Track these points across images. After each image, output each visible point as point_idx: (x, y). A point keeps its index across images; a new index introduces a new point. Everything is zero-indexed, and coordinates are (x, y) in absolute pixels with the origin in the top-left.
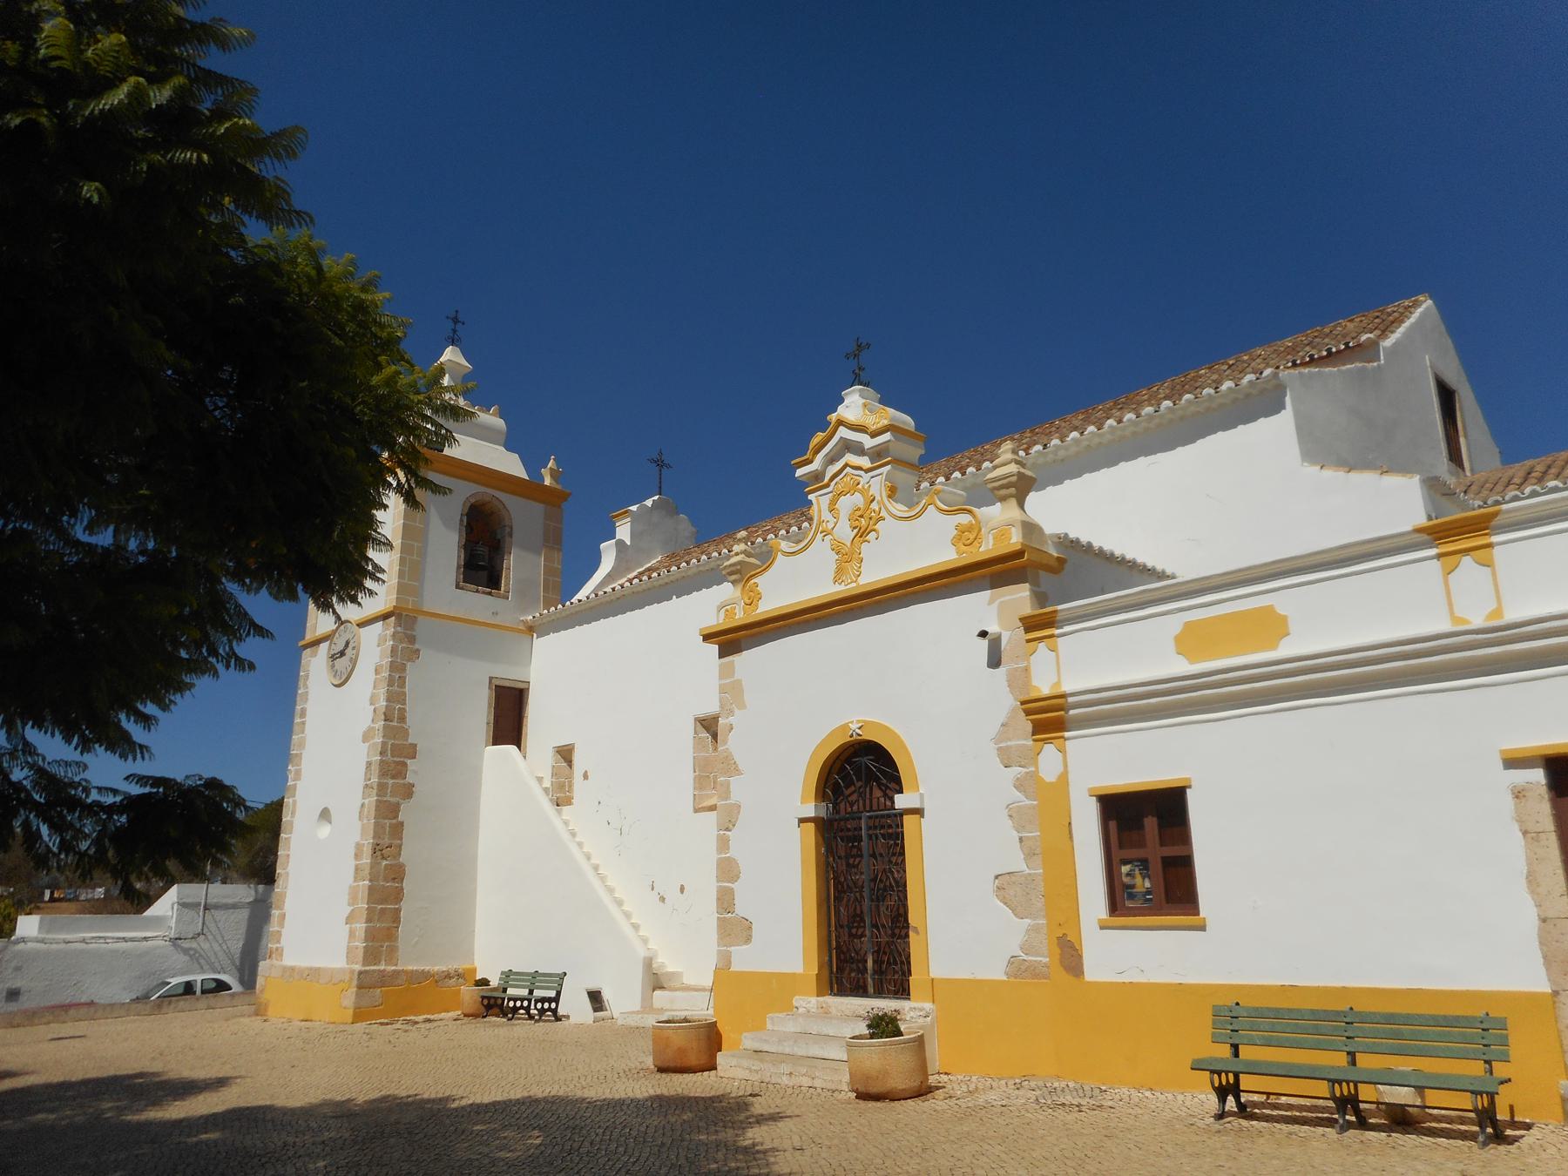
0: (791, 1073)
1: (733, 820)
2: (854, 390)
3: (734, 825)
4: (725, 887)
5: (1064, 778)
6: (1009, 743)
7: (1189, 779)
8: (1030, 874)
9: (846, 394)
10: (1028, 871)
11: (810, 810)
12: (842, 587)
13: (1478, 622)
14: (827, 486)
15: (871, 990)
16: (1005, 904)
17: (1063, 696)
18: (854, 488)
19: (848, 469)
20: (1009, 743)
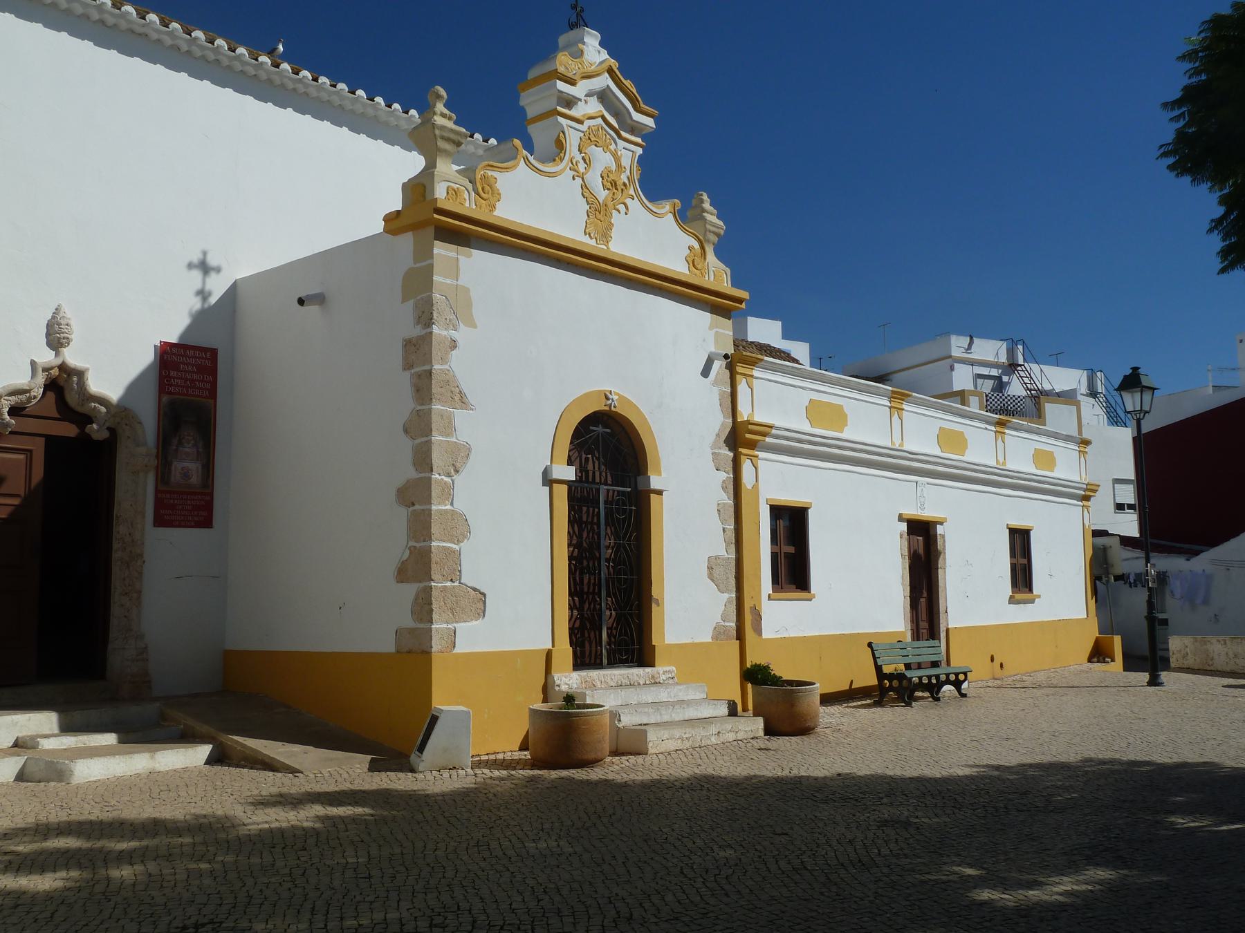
0: (719, 733)
1: (458, 465)
2: (595, 36)
3: (457, 471)
4: (449, 548)
5: (755, 487)
6: (720, 451)
7: (811, 503)
8: (729, 558)
9: (588, 33)
10: (726, 556)
11: (570, 473)
12: (593, 242)
13: (897, 447)
14: (580, 122)
15: (605, 661)
16: (713, 581)
17: (771, 427)
18: (606, 148)
19: (600, 121)
20: (720, 451)
